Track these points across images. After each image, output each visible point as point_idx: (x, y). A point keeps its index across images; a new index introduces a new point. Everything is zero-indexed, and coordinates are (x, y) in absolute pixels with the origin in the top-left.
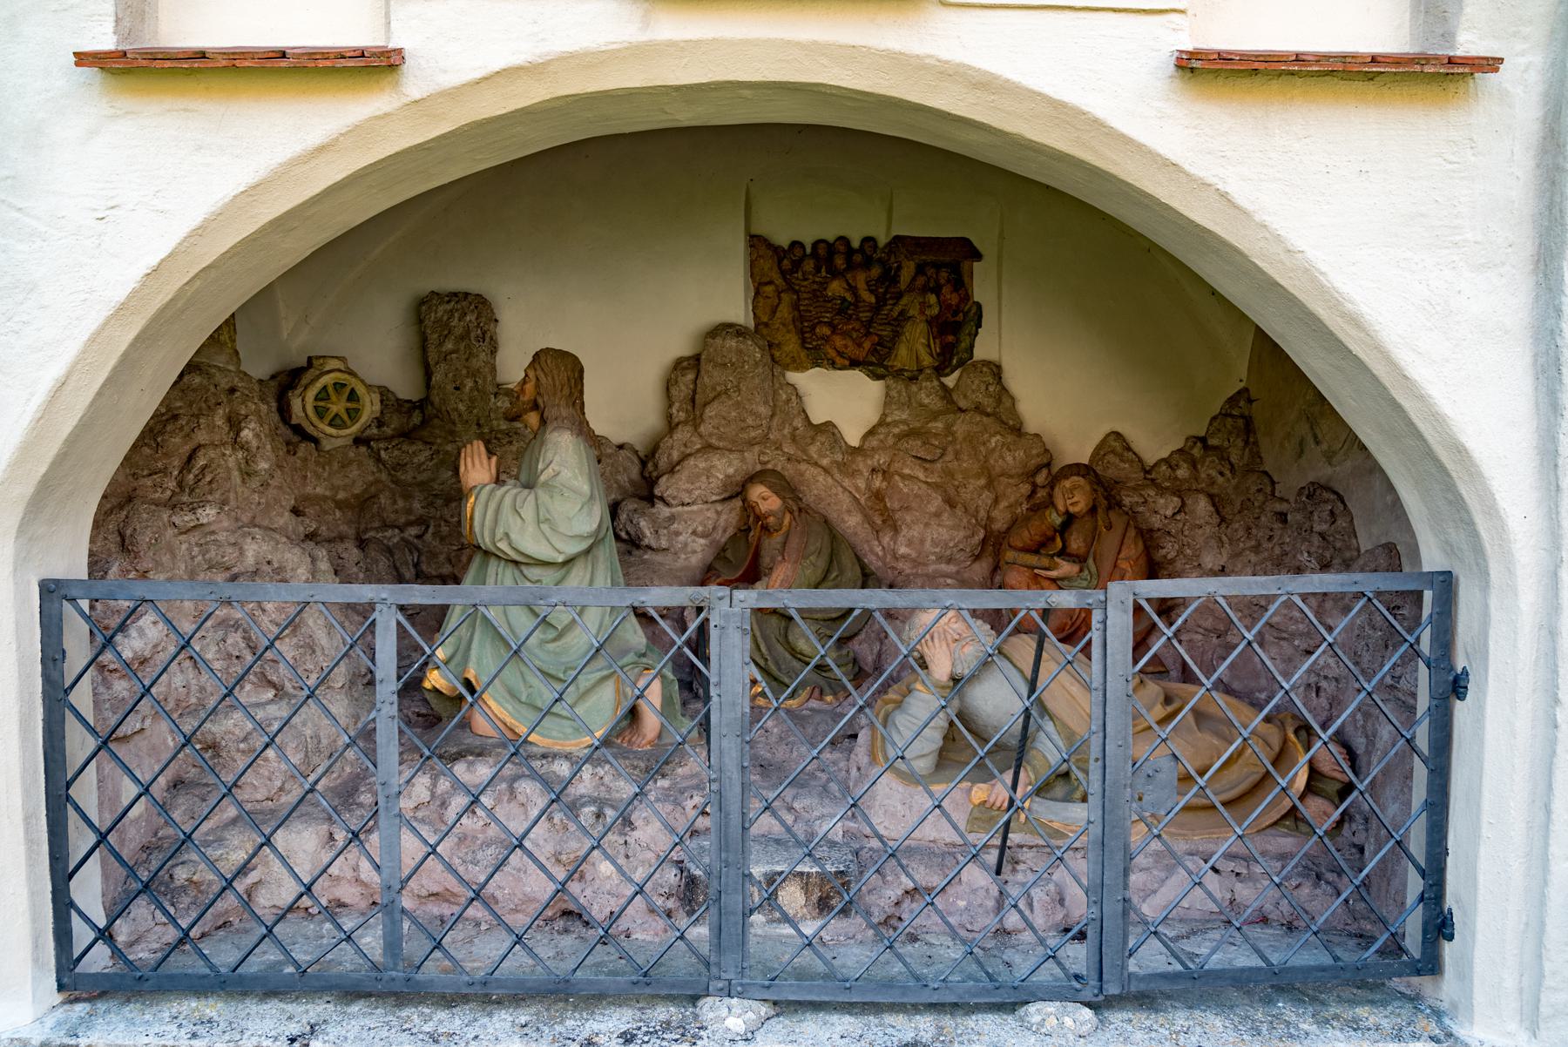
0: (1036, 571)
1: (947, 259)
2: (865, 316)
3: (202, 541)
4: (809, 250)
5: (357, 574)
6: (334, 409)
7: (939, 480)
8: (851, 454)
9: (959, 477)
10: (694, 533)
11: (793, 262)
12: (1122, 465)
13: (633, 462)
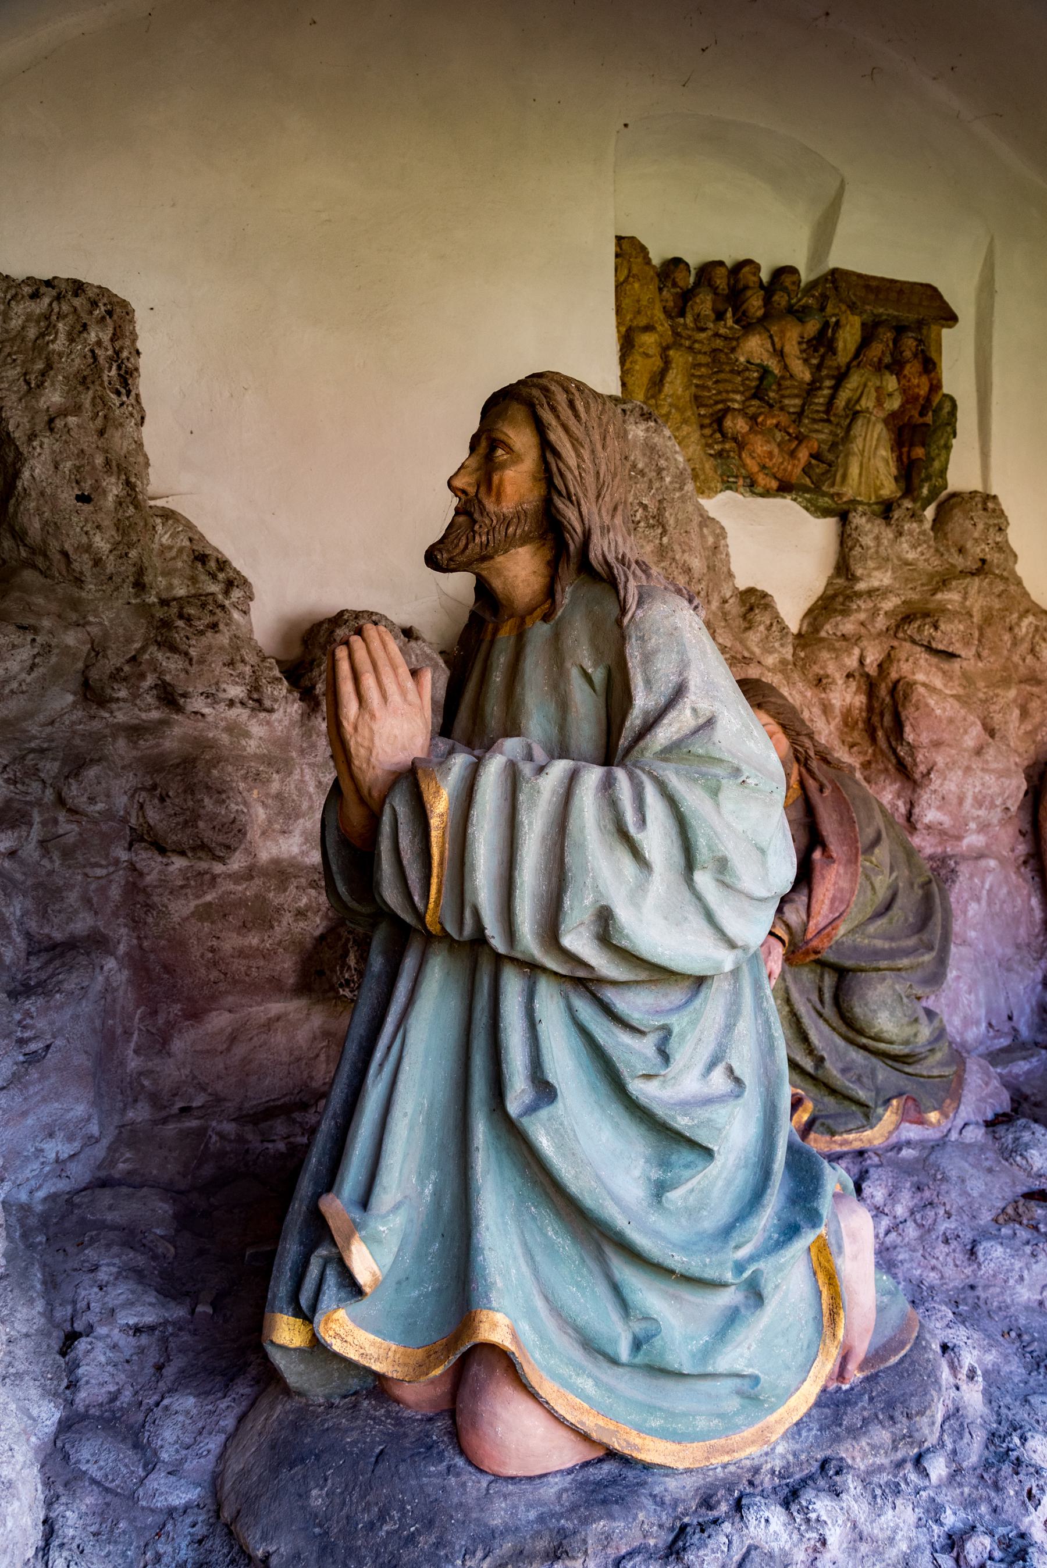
8: (804, 647)
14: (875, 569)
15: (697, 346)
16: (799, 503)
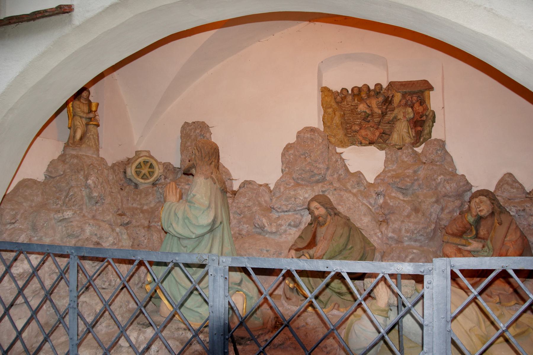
0: (459, 247)
1: (416, 90)
2: (377, 120)
3: (67, 225)
4: (350, 92)
5: (144, 241)
6: (143, 172)
7: (410, 199)
9: (422, 197)
10: (289, 225)
11: (342, 98)
12: (512, 190)
13: (266, 192)
14: (390, 164)
15: (346, 109)
16: (376, 147)
